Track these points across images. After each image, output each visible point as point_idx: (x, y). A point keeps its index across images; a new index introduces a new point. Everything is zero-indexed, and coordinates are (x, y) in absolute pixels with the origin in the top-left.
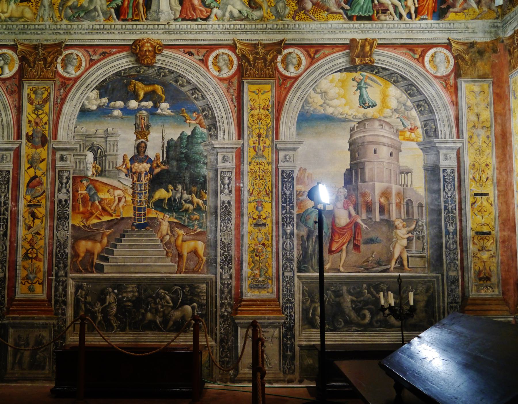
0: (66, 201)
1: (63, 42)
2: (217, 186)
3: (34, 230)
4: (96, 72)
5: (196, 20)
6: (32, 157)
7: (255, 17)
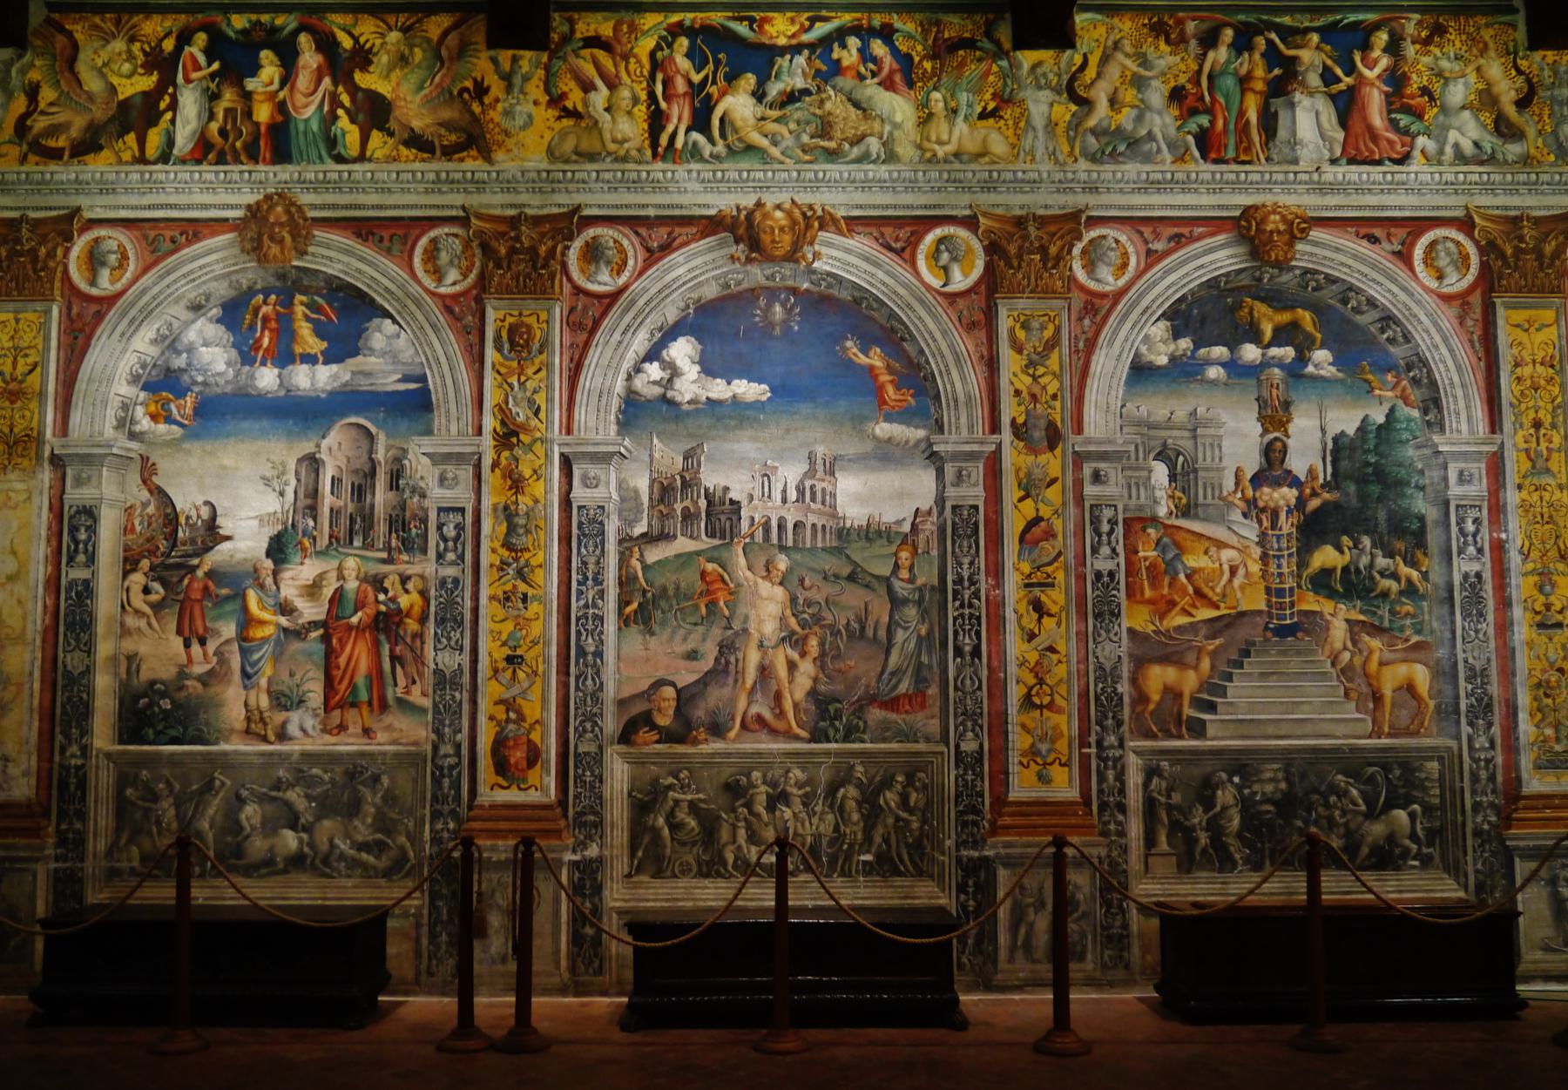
0: (1111, 574)
1: (1081, 211)
2: (1449, 539)
3: (1042, 641)
4: (1162, 278)
5: (1379, 163)
6: (1029, 475)
7: (1510, 158)
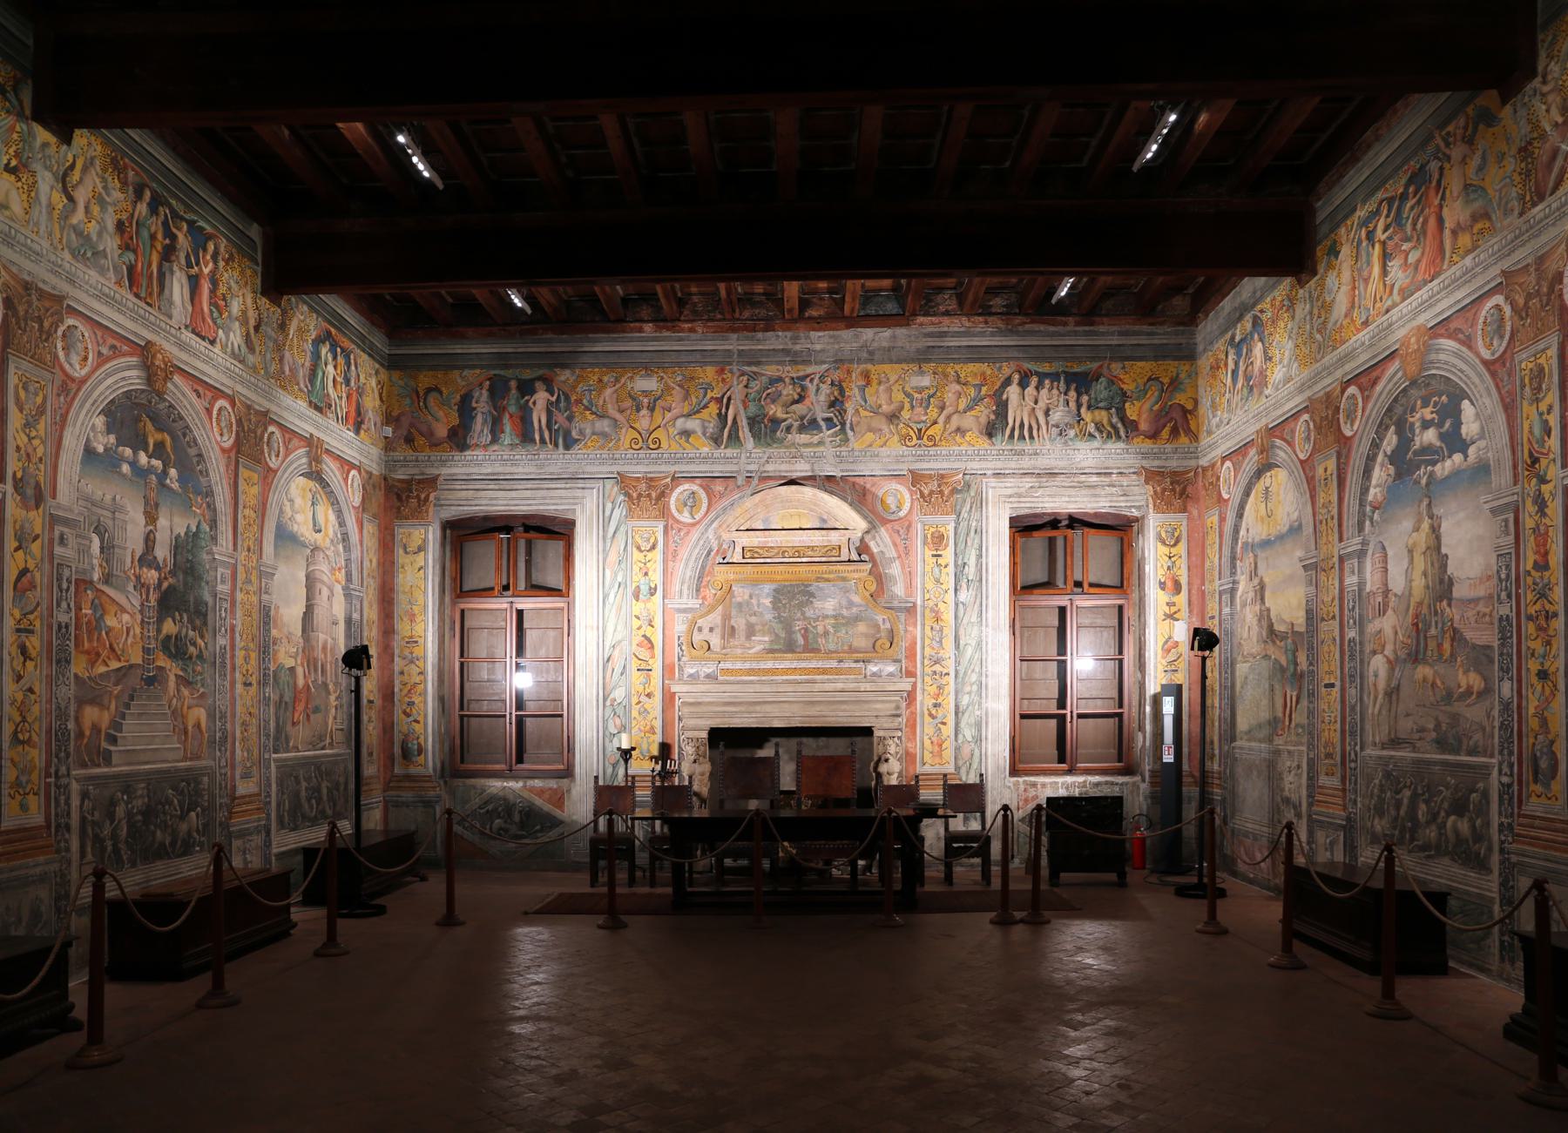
5: (203, 338)
6: (22, 527)
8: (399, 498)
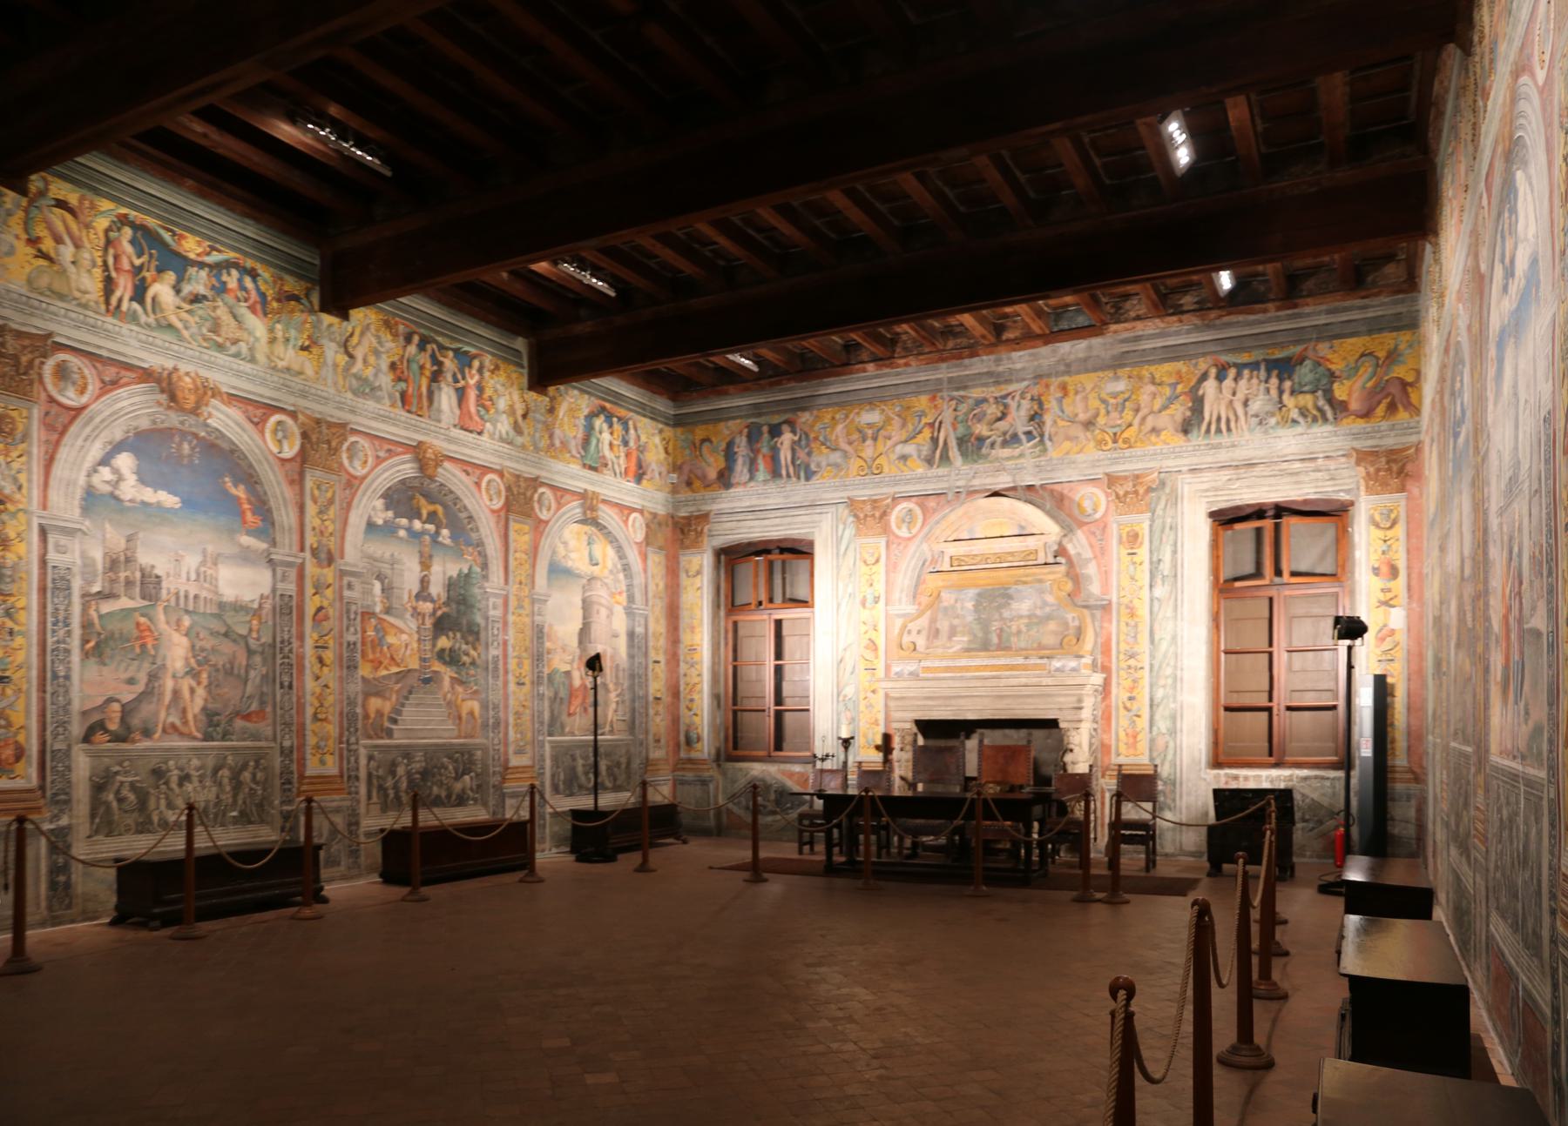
3: (322, 681)
8: (682, 531)
